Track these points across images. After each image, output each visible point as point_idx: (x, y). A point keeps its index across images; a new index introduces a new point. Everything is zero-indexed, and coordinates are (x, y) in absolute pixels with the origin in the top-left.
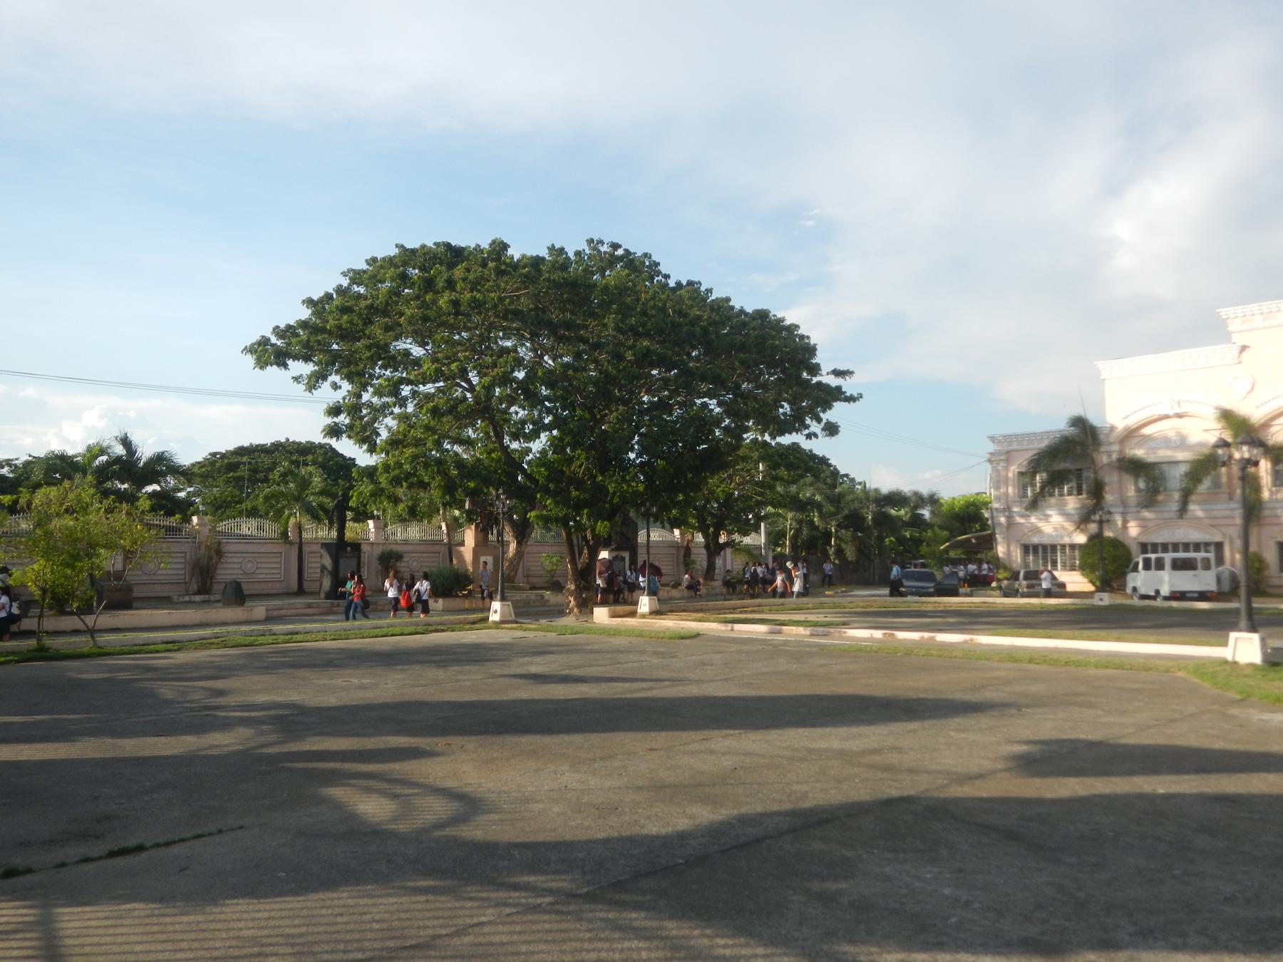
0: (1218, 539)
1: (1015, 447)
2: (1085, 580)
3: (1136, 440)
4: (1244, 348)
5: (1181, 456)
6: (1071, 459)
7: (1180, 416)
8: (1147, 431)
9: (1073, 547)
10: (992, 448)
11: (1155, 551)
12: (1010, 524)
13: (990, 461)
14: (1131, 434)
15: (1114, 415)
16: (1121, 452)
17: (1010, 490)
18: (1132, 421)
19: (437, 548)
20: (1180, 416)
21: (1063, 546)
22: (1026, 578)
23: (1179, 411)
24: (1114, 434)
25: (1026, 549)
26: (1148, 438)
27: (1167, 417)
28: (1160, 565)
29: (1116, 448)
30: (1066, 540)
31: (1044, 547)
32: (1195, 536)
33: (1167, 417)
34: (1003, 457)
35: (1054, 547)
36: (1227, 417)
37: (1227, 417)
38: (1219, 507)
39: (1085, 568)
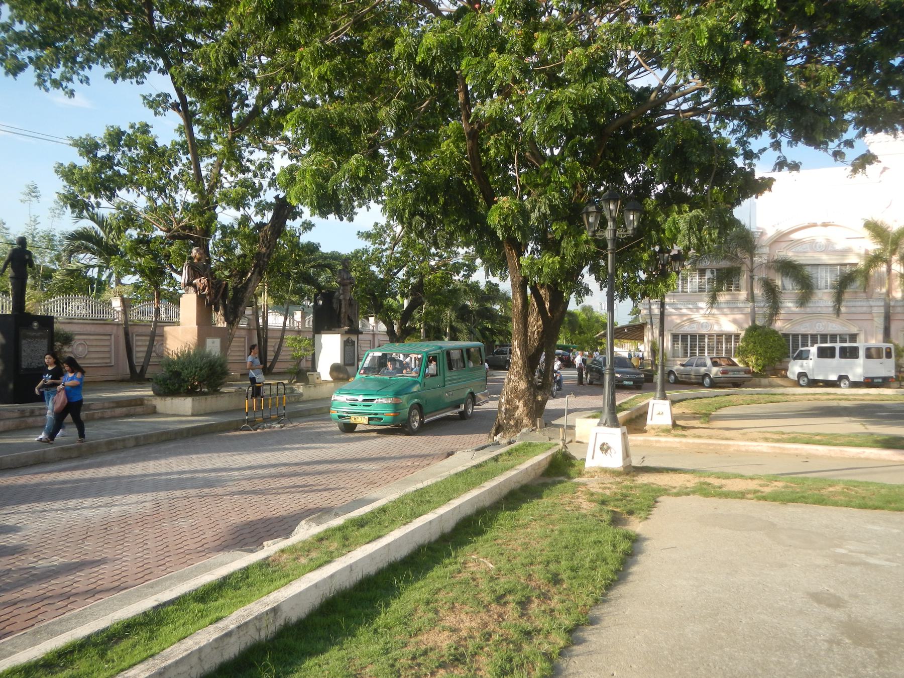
0: (854, 330)
3: (783, 245)
4: (885, 169)
5: (825, 259)
7: (825, 225)
8: (794, 236)
9: (719, 335)
14: (780, 238)
18: (784, 228)
19: (108, 329)
20: (825, 225)
21: (710, 335)
24: (765, 238)
25: (675, 337)
26: (799, 242)
27: (815, 225)
30: (716, 329)
31: (693, 337)
32: (834, 327)
33: (815, 225)
35: (702, 337)
38: (859, 304)
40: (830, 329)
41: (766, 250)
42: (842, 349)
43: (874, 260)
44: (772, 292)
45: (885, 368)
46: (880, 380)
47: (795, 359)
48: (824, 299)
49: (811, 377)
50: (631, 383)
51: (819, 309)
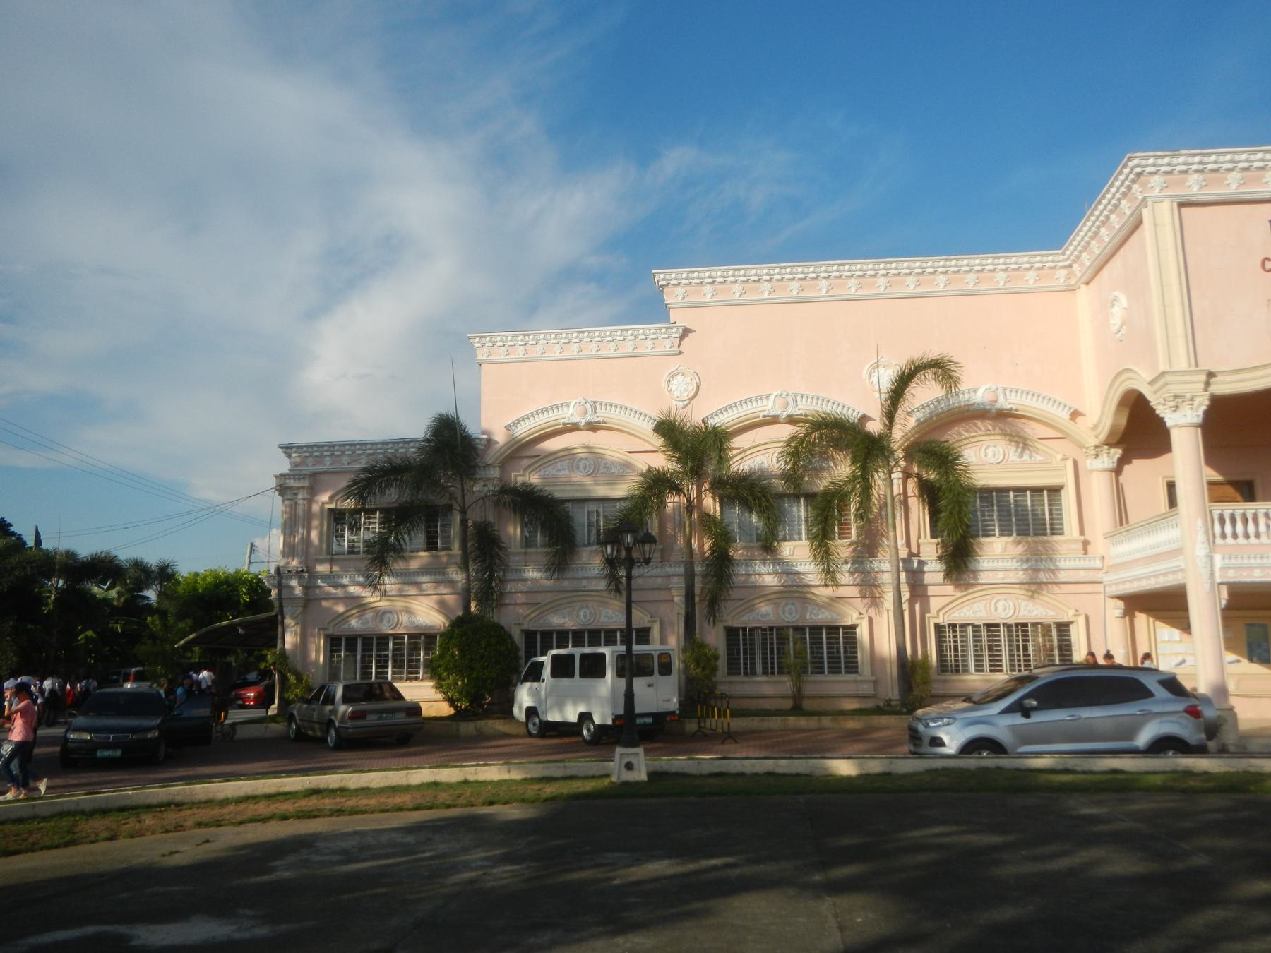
1: (327, 464)
2: (440, 696)
3: (525, 462)
4: (686, 332)
6: (430, 487)
7: (592, 427)
10: (284, 466)
11: (578, 643)
12: (310, 600)
13: (282, 489)
14: (520, 450)
15: (496, 418)
16: (500, 480)
17: (314, 535)
18: (522, 431)
20: (592, 427)
21: (397, 637)
22: (346, 700)
23: (591, 417)
25: (334, 643)
27: (574, 428)
28: (593, 668)
29: (495, 473)
33: (574, 428)
34: (306, 483)
35: (383, 639)
36: (668, 430)
37: (668, 430)
39: (434, 671)
40: (603, 619)
41: (495, 473)
42: (583, 656)
43: (658, 484)
44: (485, 550)
45: (660, 695)
46: (650, 720)
47: (525, 679)
48: (591, 562)
49: (543, 718)
50: (118, 753)
51: (584, 583)
